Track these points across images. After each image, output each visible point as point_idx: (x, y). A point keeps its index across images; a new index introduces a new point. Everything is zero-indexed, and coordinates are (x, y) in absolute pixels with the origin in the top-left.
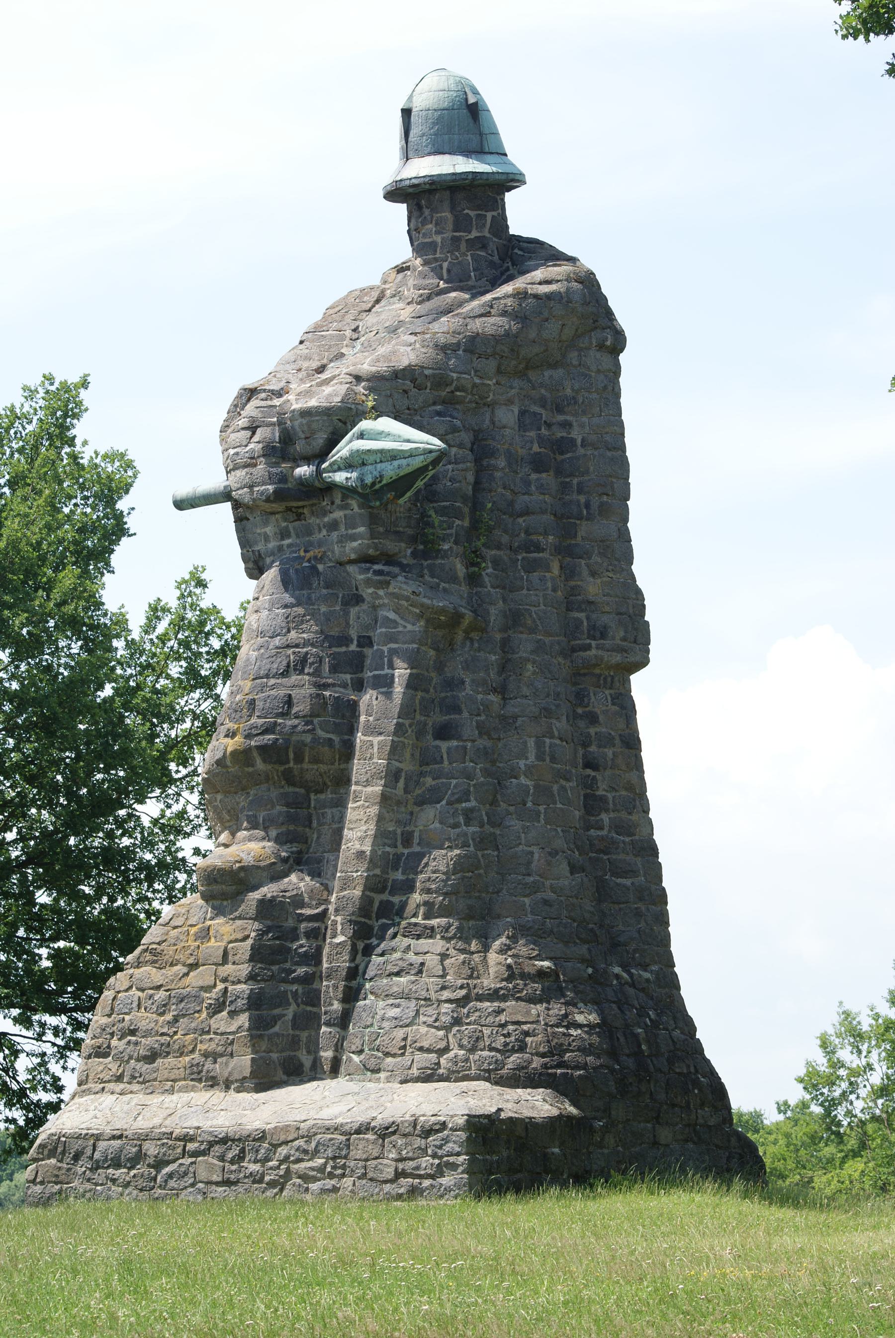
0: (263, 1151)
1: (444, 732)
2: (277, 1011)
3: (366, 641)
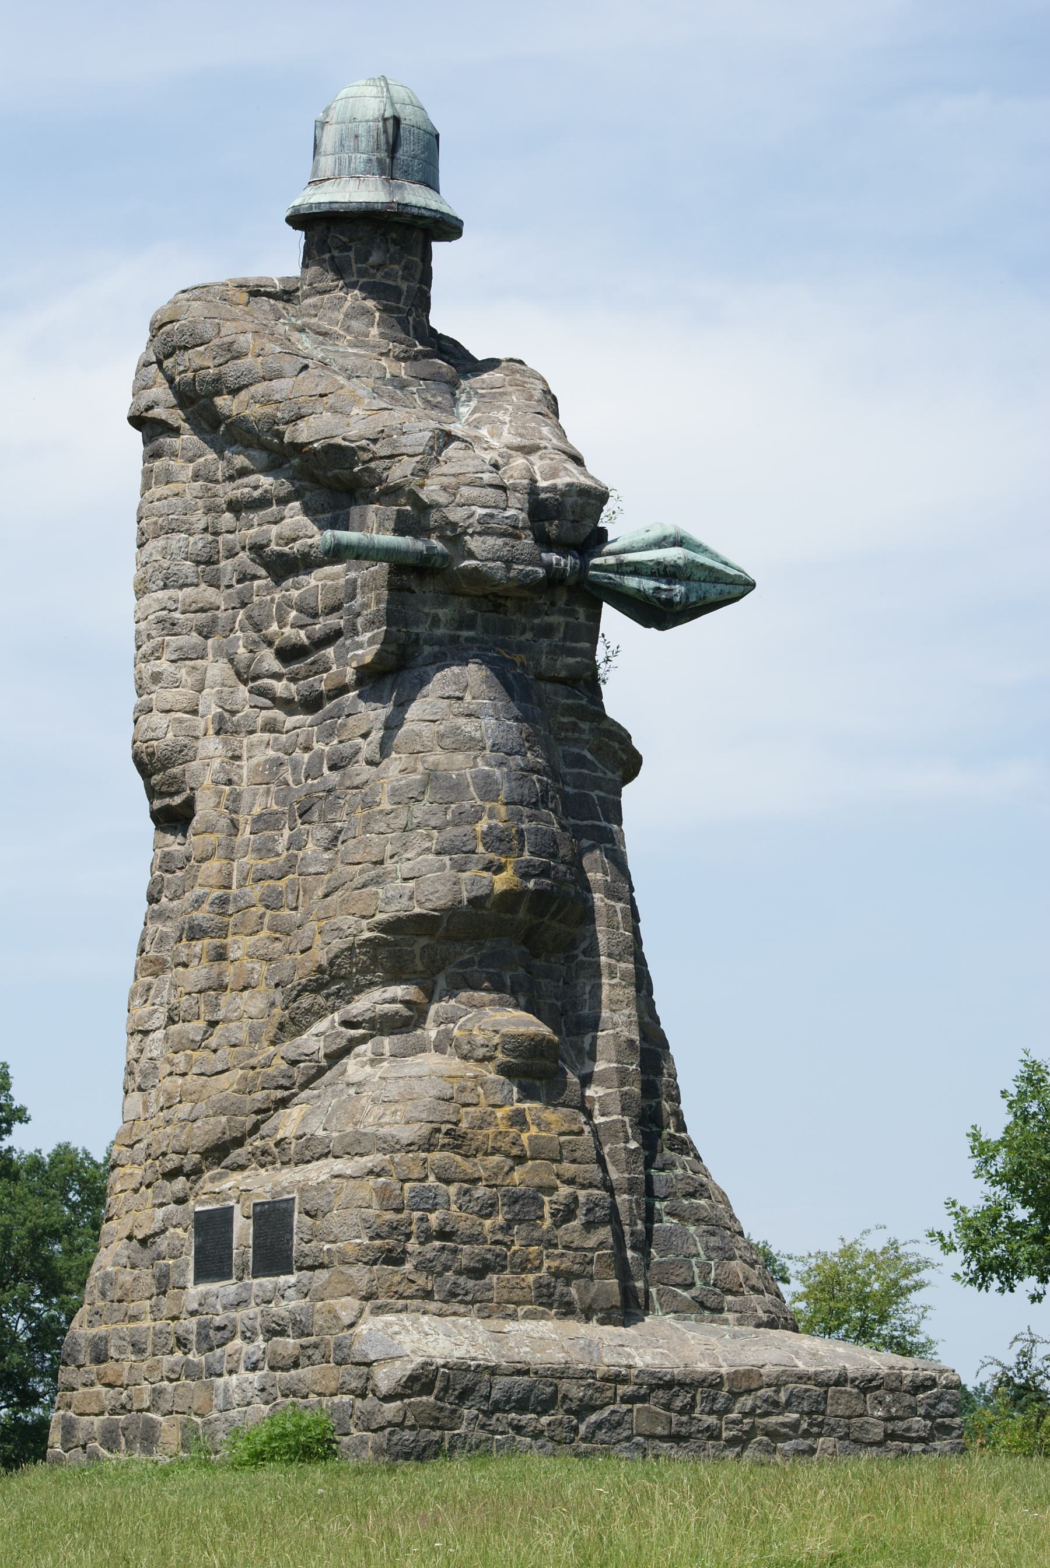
0: (722, 1400)
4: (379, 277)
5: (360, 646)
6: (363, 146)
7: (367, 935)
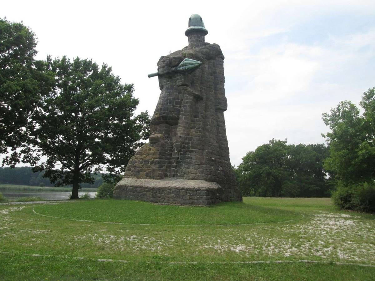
1: (195, 116)
2: (163, 165)
3: (182, 100)
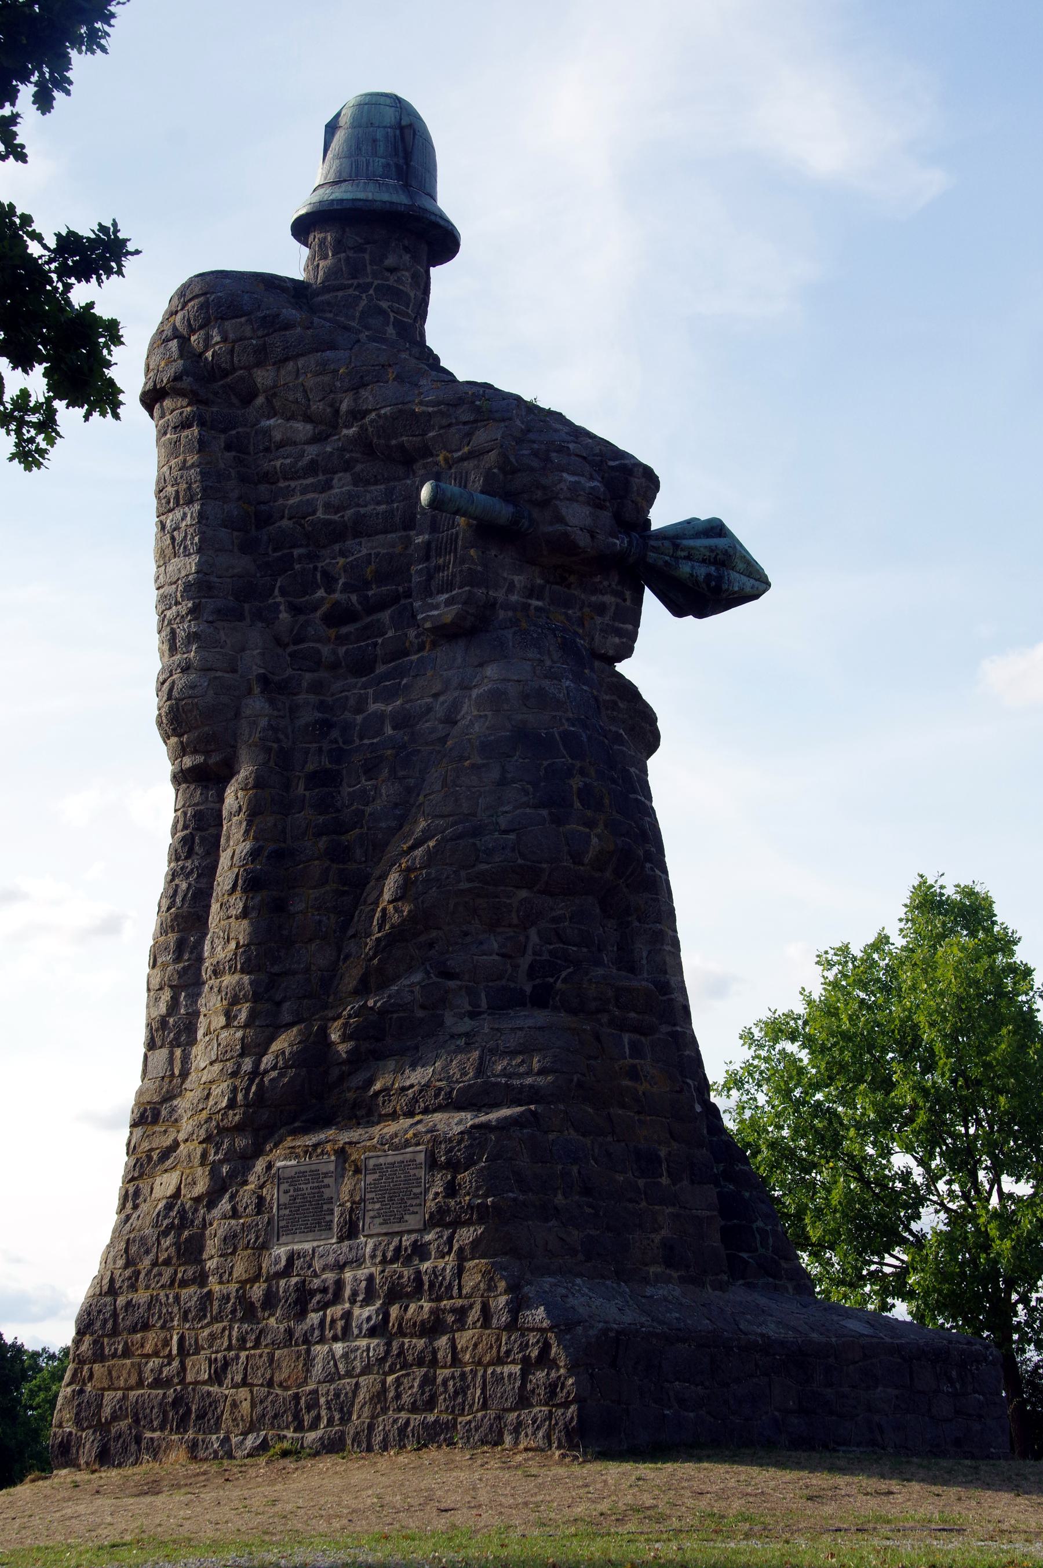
4: (392, 280)
5: (436, 607)
6: (381, 150)
7: (464, 885)
